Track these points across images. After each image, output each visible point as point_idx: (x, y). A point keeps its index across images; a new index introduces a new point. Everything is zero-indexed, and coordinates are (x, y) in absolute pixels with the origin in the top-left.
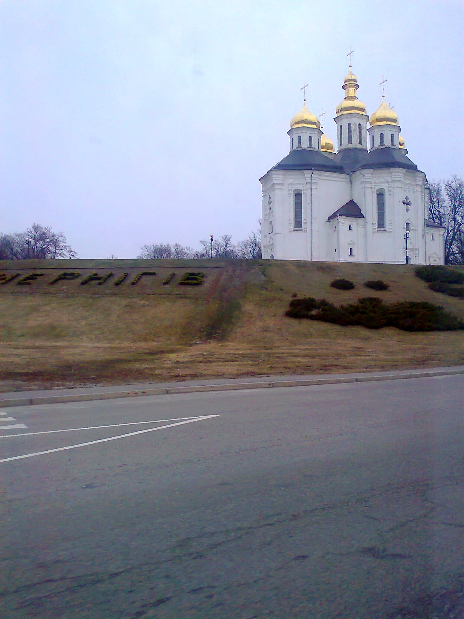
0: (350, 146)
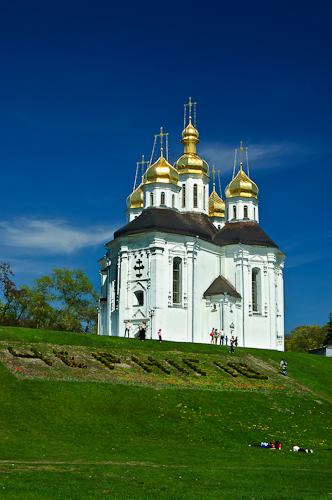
0: (196, 210)
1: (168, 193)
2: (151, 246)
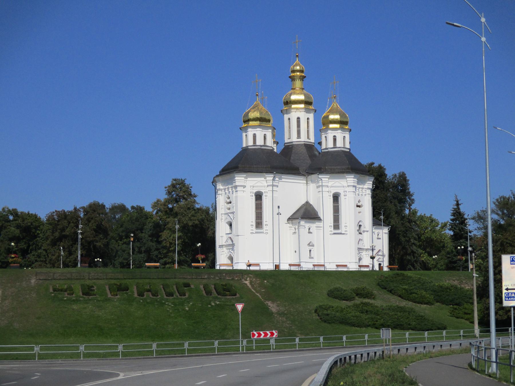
1: (260, 133)
2: (234, 184)
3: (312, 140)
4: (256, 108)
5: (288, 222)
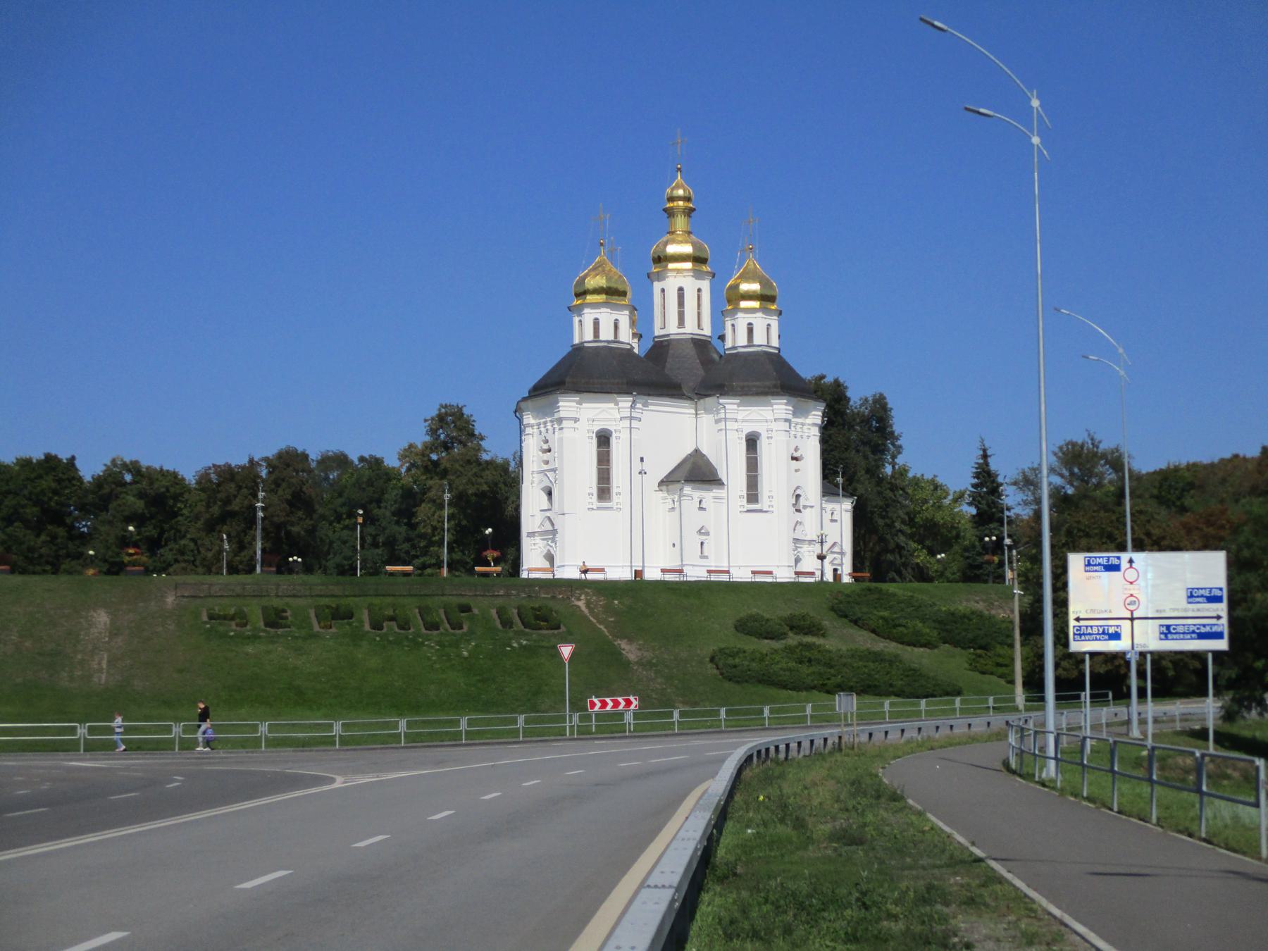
1: (606, 317)
2: (556, 416)
3: (707, 331)
4: (599, 269)
5: (661, 488)
